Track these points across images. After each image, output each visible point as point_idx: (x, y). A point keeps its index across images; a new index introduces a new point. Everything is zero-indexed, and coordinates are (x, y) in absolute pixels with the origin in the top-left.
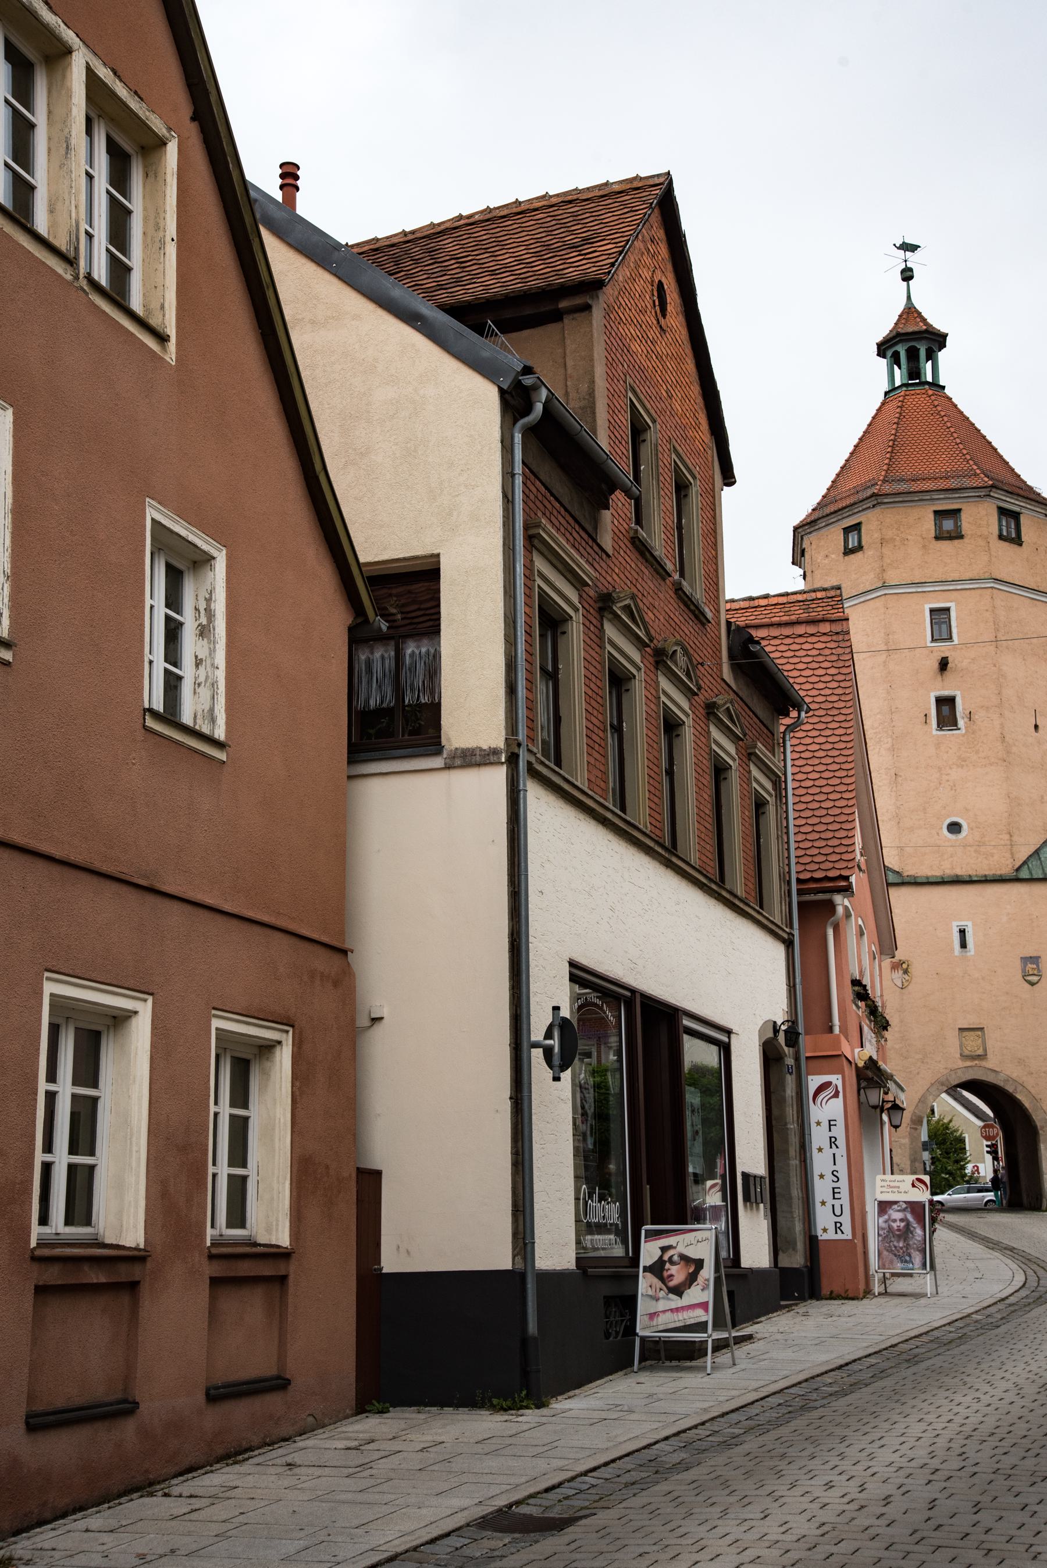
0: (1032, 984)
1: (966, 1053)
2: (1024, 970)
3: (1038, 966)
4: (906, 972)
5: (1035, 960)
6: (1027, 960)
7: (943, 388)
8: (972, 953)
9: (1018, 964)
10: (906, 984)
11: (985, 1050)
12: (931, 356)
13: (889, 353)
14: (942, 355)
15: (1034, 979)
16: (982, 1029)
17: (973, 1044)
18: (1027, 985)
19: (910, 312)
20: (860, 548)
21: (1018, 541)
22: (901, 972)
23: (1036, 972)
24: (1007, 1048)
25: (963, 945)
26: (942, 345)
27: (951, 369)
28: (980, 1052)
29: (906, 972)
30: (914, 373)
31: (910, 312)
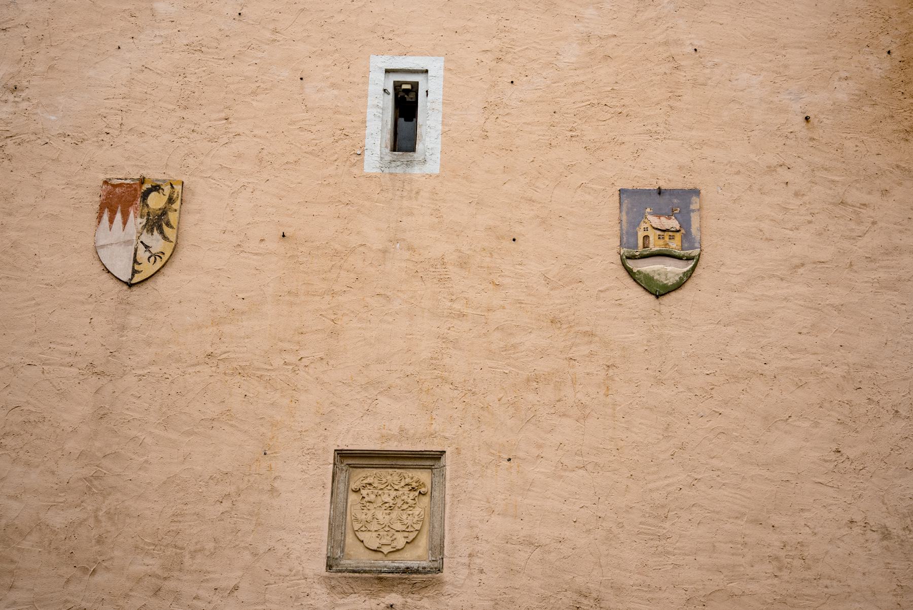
0: (659, 291)
1: (357, 556)
2: (627, 236)
3: (685, 224)
4: (157, 222)
5: (677, 201)
6: (635, 200)
8: (434, 167)
9: (608, 213)
10: (147, 269)
11: (437, 548)
15: (670, 270)
16: (431, 459)
17: (384, 517)
18: (636, 293)
22: (136, 222)
23: (675, 246)
24: (530, 543)
25: (403, 140)
28: (416, 556)
29: (157, 222)
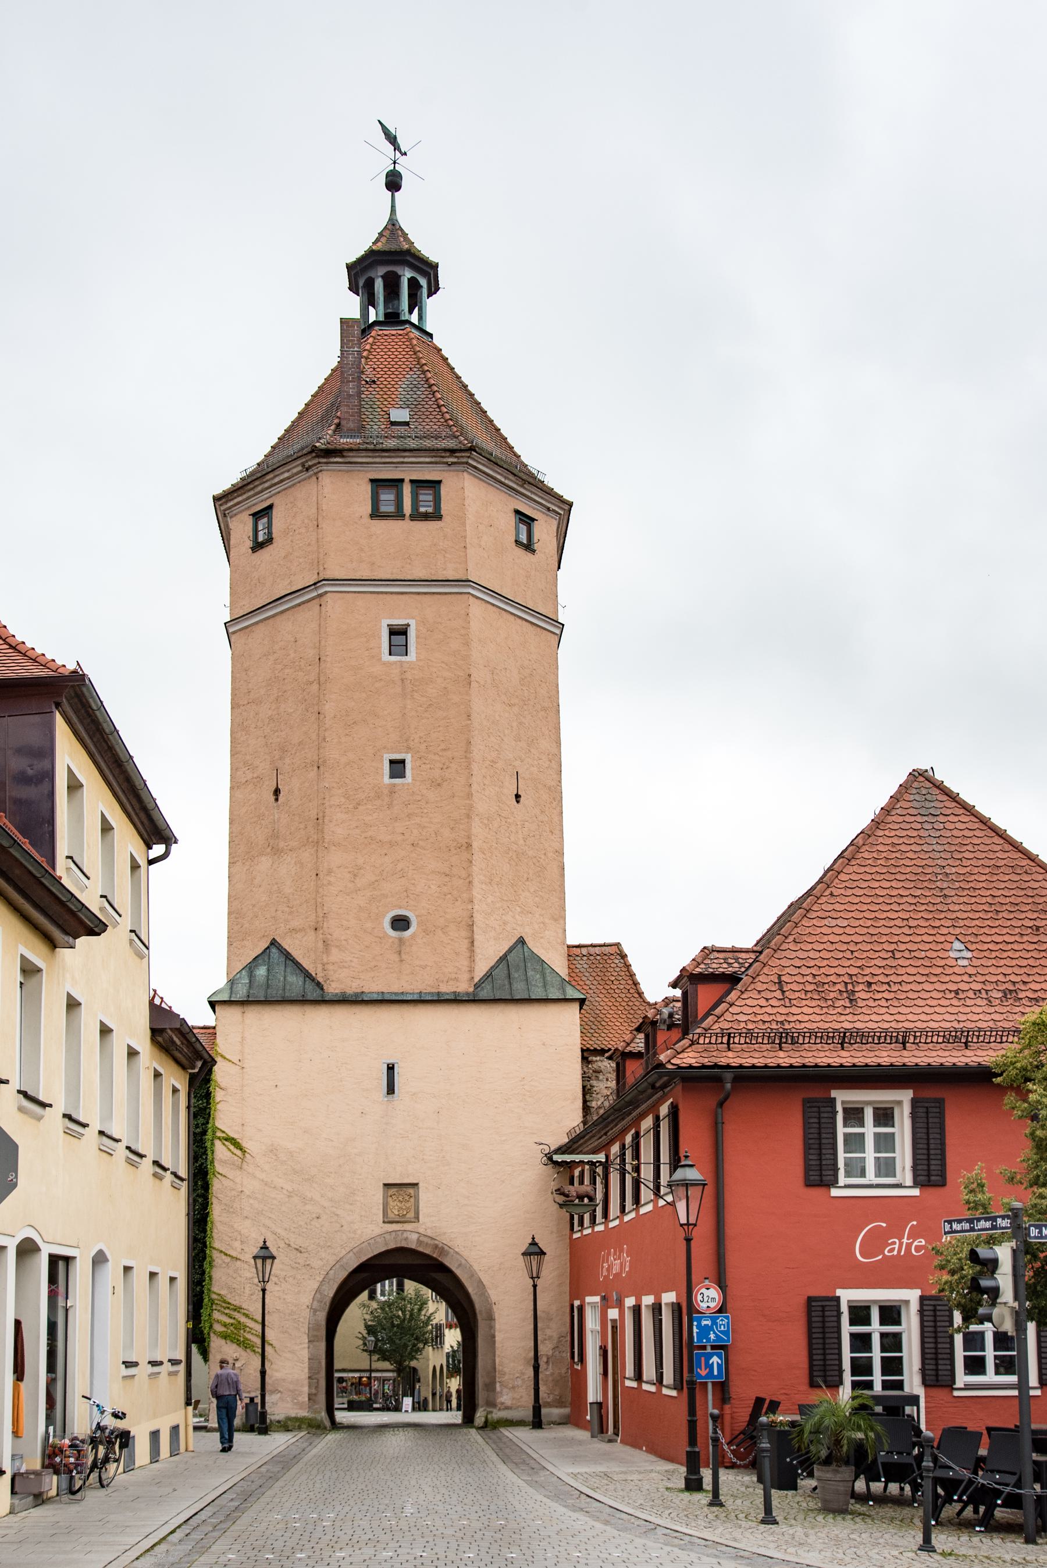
7: (431, 335)
12: (415, 302)
13: (361, 283)
14: (431, 304)
19: (393, 228)
20: (270, 540)
21: (528, 547)
26: (434, 289)
27: (445, 319)
30: (392, 318)
31: (393, 228)
